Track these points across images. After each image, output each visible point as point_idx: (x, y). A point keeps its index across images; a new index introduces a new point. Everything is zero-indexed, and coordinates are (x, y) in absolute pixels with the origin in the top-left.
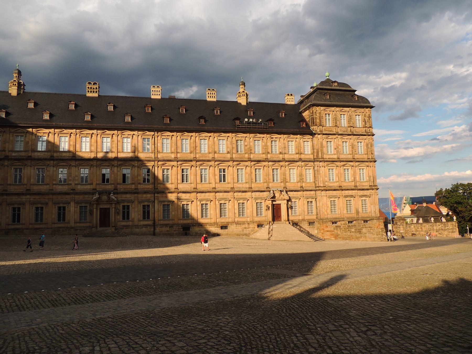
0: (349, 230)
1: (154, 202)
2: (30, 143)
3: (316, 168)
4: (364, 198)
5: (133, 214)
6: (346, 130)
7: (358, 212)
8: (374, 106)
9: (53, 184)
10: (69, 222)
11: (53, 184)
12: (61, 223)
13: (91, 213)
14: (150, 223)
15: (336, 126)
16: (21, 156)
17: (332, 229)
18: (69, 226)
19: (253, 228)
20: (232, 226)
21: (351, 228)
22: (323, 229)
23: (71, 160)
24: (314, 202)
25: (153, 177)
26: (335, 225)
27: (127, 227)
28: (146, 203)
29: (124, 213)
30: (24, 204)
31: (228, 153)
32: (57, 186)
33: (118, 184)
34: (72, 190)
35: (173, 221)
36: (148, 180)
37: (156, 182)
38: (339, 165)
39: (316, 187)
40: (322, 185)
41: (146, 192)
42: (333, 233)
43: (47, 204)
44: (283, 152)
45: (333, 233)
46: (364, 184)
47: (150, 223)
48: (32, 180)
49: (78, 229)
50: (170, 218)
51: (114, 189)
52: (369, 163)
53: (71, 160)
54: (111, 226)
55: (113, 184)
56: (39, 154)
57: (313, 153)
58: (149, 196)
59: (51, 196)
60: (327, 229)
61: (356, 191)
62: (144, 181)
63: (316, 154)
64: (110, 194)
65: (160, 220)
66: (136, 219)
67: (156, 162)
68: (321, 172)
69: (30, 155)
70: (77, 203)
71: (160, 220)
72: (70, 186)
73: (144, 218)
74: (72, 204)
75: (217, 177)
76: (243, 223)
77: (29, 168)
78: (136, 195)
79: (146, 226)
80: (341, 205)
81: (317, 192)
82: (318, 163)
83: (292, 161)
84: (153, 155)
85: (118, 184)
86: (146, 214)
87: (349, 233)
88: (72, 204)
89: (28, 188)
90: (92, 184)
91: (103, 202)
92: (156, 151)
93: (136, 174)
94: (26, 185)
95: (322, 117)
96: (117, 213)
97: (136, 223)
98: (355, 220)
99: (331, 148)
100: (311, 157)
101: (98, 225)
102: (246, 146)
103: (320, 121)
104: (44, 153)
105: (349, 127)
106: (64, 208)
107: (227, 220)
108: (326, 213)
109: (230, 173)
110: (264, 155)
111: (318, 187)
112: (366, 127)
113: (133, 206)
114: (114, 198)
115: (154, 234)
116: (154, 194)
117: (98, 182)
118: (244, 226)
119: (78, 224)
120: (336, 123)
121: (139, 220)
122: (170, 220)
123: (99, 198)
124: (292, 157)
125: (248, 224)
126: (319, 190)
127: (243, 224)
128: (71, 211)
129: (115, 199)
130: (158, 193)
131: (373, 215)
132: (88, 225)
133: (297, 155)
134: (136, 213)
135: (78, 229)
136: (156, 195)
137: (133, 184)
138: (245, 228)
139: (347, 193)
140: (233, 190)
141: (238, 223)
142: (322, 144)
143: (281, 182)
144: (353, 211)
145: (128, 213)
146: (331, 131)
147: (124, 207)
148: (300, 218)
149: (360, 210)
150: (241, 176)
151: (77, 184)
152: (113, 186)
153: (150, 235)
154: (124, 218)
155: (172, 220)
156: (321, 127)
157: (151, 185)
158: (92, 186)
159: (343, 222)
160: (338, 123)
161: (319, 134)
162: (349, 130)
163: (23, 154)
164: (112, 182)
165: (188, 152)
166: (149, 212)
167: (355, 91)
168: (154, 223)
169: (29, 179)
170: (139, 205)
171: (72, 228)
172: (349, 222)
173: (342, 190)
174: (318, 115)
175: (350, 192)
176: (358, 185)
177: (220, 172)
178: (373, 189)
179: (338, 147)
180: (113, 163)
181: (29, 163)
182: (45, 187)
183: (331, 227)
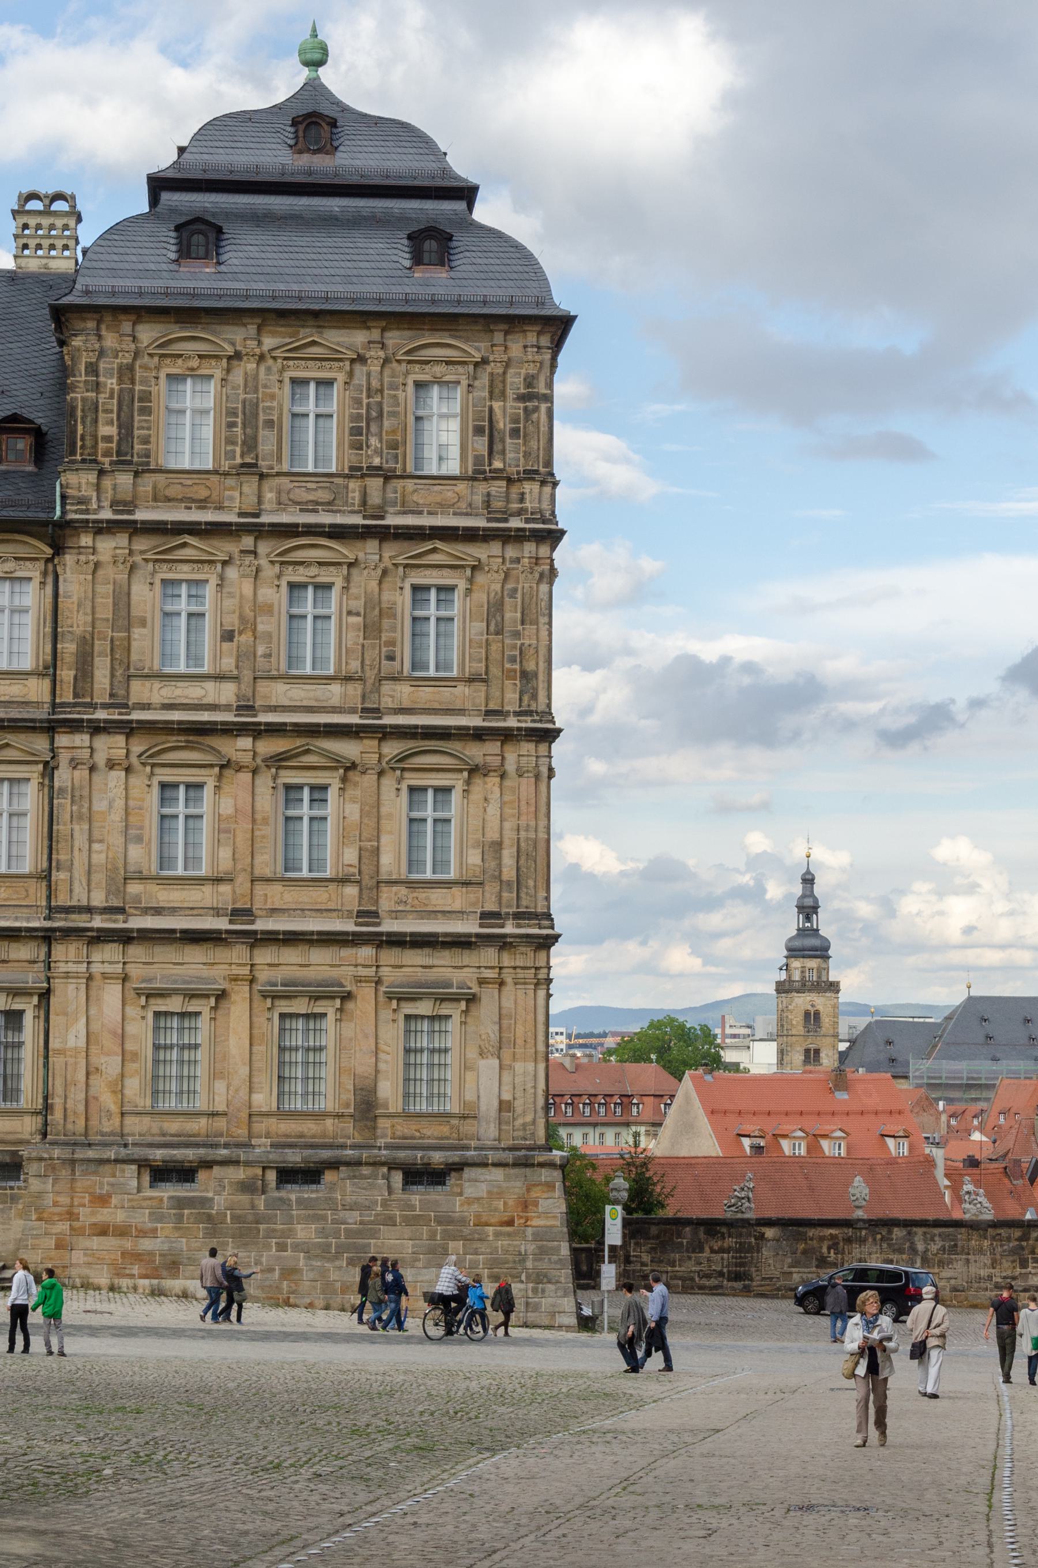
3: (63, 776)
6: (324, 496)
7: (366, 1108)
15: (249, 469)
17: (142, 1218)
22: (71, 1216)
26: (169, 1191)
38: (246, 759)
39: (52, 911)
40: (98, 899)
52: (493, 747)
57: (50, 670)
60: (104, 1215)
61: (366, 952)
68: (100, 805)
80: (237, 1043)
81: (59, 951)
82: (82, 739)
95: (146, 397)
99: (186, 635)
100: (37, 690)
103: (126, 429)
105: (356, 472)
108: (108, 1101)
111: (68, 910)
112: (497, 475)
120: (250, 444)
126: (68, 933)
131: (489, 1131)
142: (122, 599)
146: (202, 504)
149: (388, 1091)
156: (125, 479)
161: (103, 529)
162: (356, 496)
174: (111, 383)
178: (504, 943)
179: (249, 625)
183: (131, 1199)
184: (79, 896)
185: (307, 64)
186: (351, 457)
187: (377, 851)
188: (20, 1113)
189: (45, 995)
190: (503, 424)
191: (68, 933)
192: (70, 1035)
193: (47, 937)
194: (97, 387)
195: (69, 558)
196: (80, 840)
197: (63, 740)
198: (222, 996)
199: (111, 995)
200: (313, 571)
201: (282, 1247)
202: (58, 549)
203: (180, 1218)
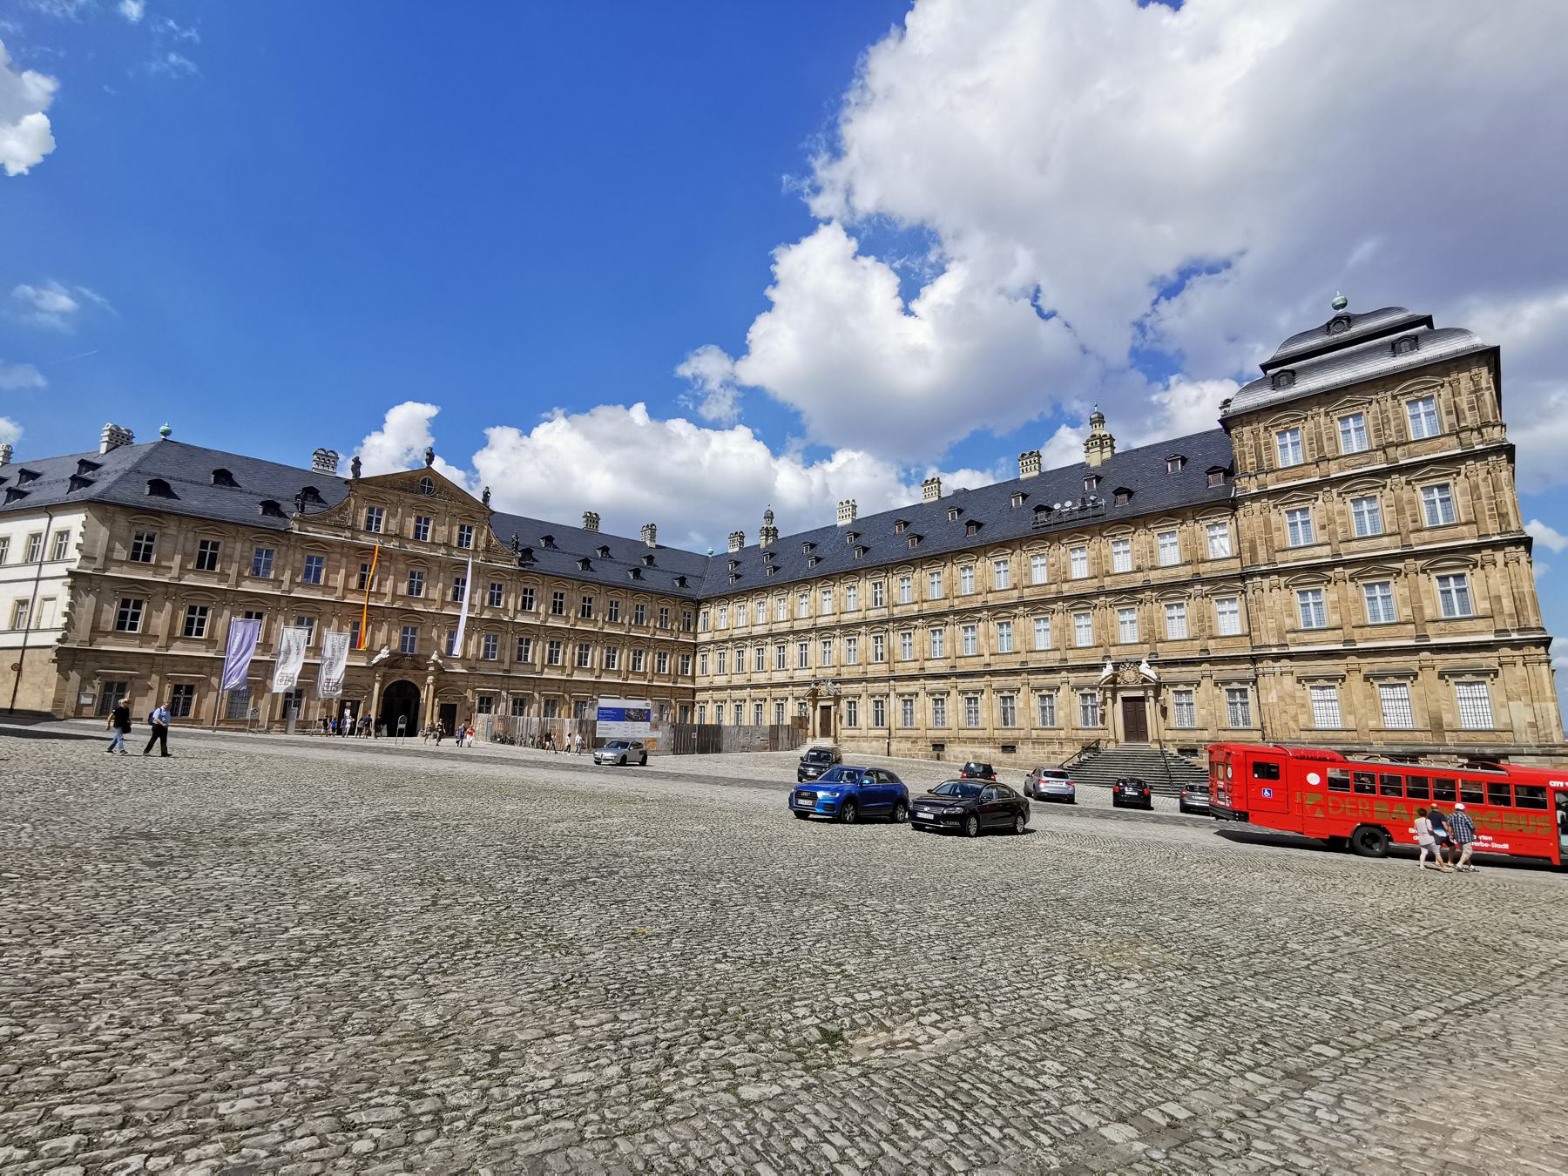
14: (885, 733)
40: (1273, 641)
47: (885, 733)
61: (1425, 655)
70: (797, 699)
76: (1050, 741)
79: (877, 738)
86: (879, 719)
97: (864, 733)
107: (1016, 734)
118: (1050, 748)
120: (1321, 449)
124: (1173, 572)
141: (1037, 742)
142: (1267, 523)
146: (1301, 478)
179: (1331, 521)
184: (1265, 641)
187: (1421, 608)
189: (1255, 682)
190: (1465, 406)
192: (1272, 697)
193: (1254, 660)
196: (1262, 619)
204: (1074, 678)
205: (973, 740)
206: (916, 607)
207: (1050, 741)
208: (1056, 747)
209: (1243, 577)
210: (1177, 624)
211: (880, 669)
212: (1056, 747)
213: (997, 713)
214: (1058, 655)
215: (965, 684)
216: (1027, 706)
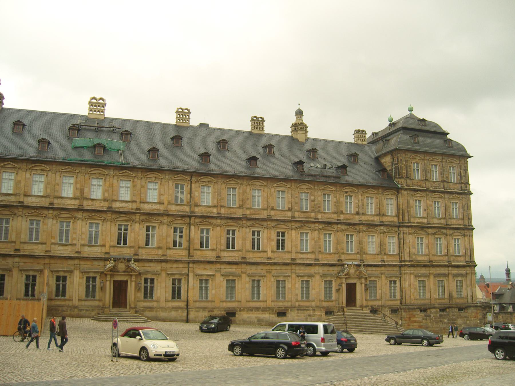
0: (441, 321)
1: (188, 275)
2: (23, 184)
3: (401, 236)
4: (459, 278)
5: (159, 291)
6: (438, 185)
7: (451, 296)
8: (471, 155)
9: (52, 244)
10: (70, 300)
11: (52, 244)
12: (61, 300)
13: (103, 289)
14: (183, 304)
16: (9, 201)
17: (421, 319)
18: (70, 303)
19: (319, 315)
20: (292, 313)
21: (443, 318)
23: (77, 210)
24: (398, 283)
25: (188, 239)
26: (423, 314)
27: (151, 309)
28: (177, 277)
29: (146, 288)
30: (10, 270)
31: (290, 209)
32: (57, 246)
33: (139, 247)
34: (76, 252)
35: (213, 304)
36: (180, 245)
37: (191, 246)
40: (408, 259)
41: (177, 261)
42: (422, 324)
43: (41, 271)
44: (361, 212)
45: (422, 324)
46: (459, 259)
48: (23, 236)
49: (83, 310)
50: (210, 298)
51: (135, 255)
53: (77, 210)
54: (128, 306)
55: (133, 247)
56: (34, 199)
57: (398, 216)
58: (181, 266)
59: (47, 261)
61: (450, 269)
62: (175, 244)
63: (401, 217)
64: (129, 260)
65: (196, 301)
66: (162, 299)
67: (192, 219)
69: (21, 200)
70: (83, 272)
71: (196, 301)
72: (74, 248)
73: (173, 297)
74: (77, 273)
75: (274, 243)
76: (307, 309)
77: (20, 219)
78: (164, 264)
79: (176, 309)
80: (432, 286)
81: (403, 269)
82: (405, 229)
83: (371, 226)
84: (187, 208)
85: (139, 247)
86: (176, 293)
87: (440, 325)
88: (77, 273)
89: (17, 247)
90: (103, 246)
91: (118, 272)
92: (193, 203)
93: (165, 235)
94: (15, 242)
95: (410, 166)
96: (138, 289)
97: (163, 304)
98: (449, 308)
101: (111, 306)
102: (313, 201)
104: (40, 199)
106: (65, 278)
107: (286, 304)
109: (292, 238)
110: (335, 215)
113: (159, 280)
114: (135, 267)
115: (187, 321)
116: (189, 263)
117: (112, 244)
118: (307, 313)
119: (83, 303)
120: (426, 176)
121: (167, 301)
122: (208, 302)
123: (114, 267)
124: (372, 218)
125: (314, 310)
126: (405, 266)
127: (307, 310)
128: (75, 282)
129: (137, 269)
130: (194, 262)
132: (97, 303)
133: (378, 218)
134: (162, 289)
135: (83, 310)
136: (191, 265)
137: (159, 248)
138: (309, 316)
139: (439, 270)
140: (293, 263)
141: (300, 309)
142: (408, 203)
143: (357, 254)
144: (447, 296)
145: (152, 289)
147: (146, 280)
148: (380, 303)
149: (455, 294)
150: (300, 243)
151: (83, 245)
152: (133, 249)
153: (181, 321)
154: (145, 296)
155: (212, 302)
157: (184, 251)
158: (103, 248)
159: (433, 310)
160: (429, 175)
161: (406, 189)
162: (442, 186)
163: (13, 198)
164: (132, 245)
165: (237, 205)
166: (179, 289)
167: (448, 134)
168: (187, 305)
169: (19, 234)
170: (168, 279)
171: (76, 307)
172: (441, 310)
173: (433, 266)
174: (404, 163)
175: (443, 270)
176: (452, 260)
177: (278, 236)
180: (134, 217)
181: (20, 211)
182: (40, 247)
183: (419, 316)
185: (409, 111)
186: (441, 179)
188: (397, 300)
189: (400, 277)
191: (405, 266)
193: (400, 266)
194: (402, 164)
195: (400, 195)
197: (401, 229)
198: (429, 277)
199: (412, 277)
200: (437, 199)
201: (442, 324)
202: (398, 193)
203: (426, 319)
204: (320, 270)
205: (257, 309)
206: (215, 211)
207: (307, 309)
208: (311, 312)
209: (399, 227)
210: (372, 245)
211: (181, 254)
212: (311, 312)
213: (274, 290)
214: (313, 256)
215: (252, 270)
216: (293, 287)
